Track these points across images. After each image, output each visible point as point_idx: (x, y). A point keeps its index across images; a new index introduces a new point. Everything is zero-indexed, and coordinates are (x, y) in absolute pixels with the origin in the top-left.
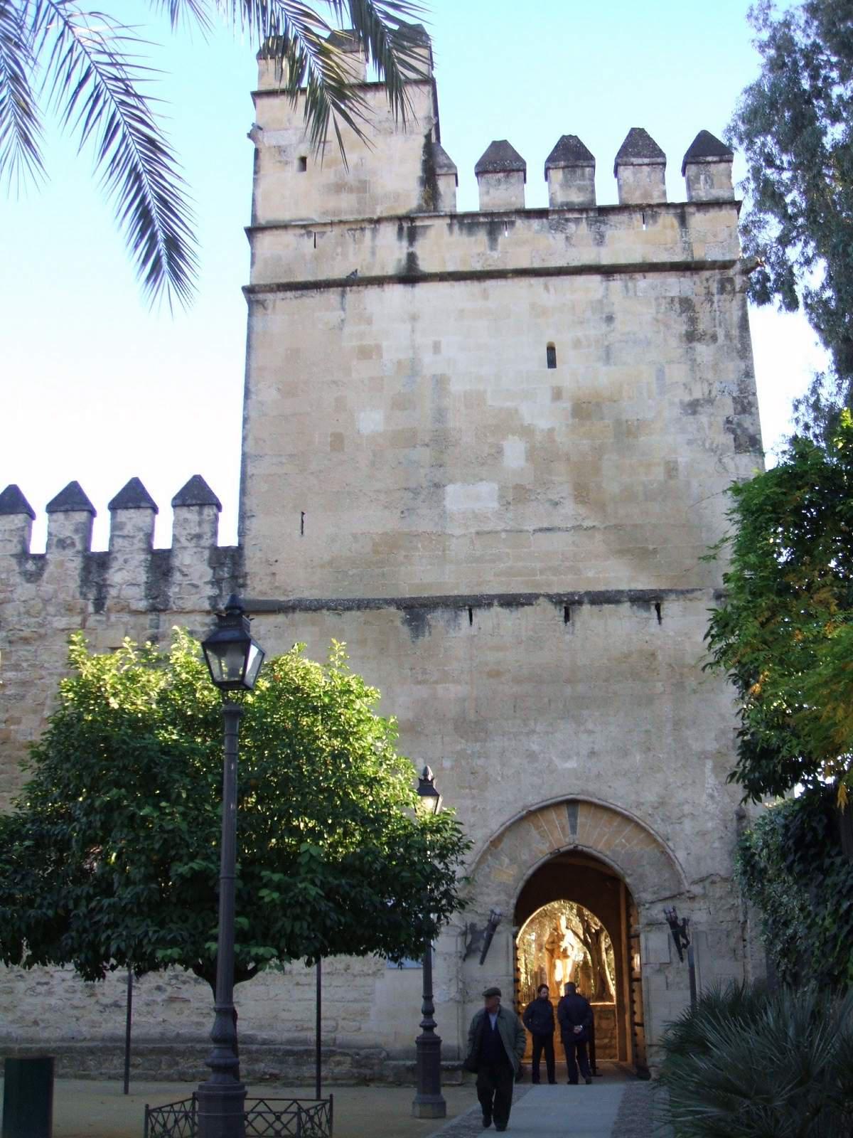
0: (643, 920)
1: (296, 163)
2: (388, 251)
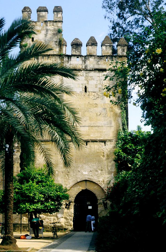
0: (98, 203)
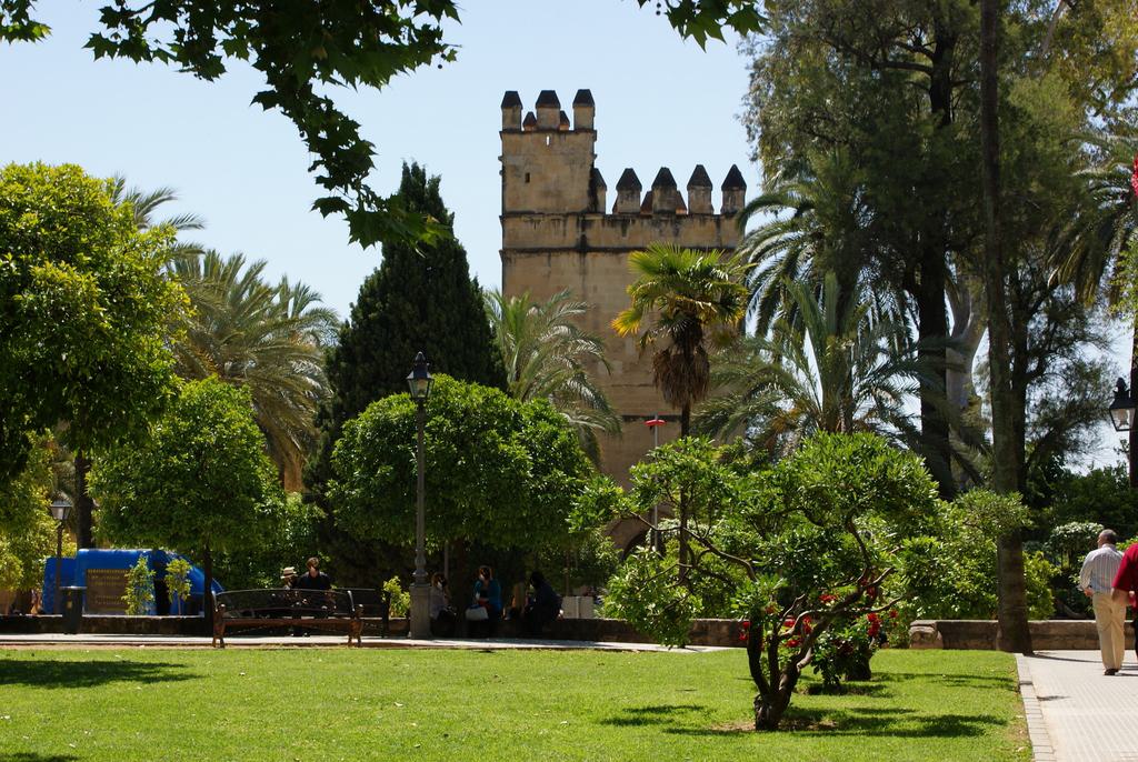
1: (524, 177)
2: (571, 234)
